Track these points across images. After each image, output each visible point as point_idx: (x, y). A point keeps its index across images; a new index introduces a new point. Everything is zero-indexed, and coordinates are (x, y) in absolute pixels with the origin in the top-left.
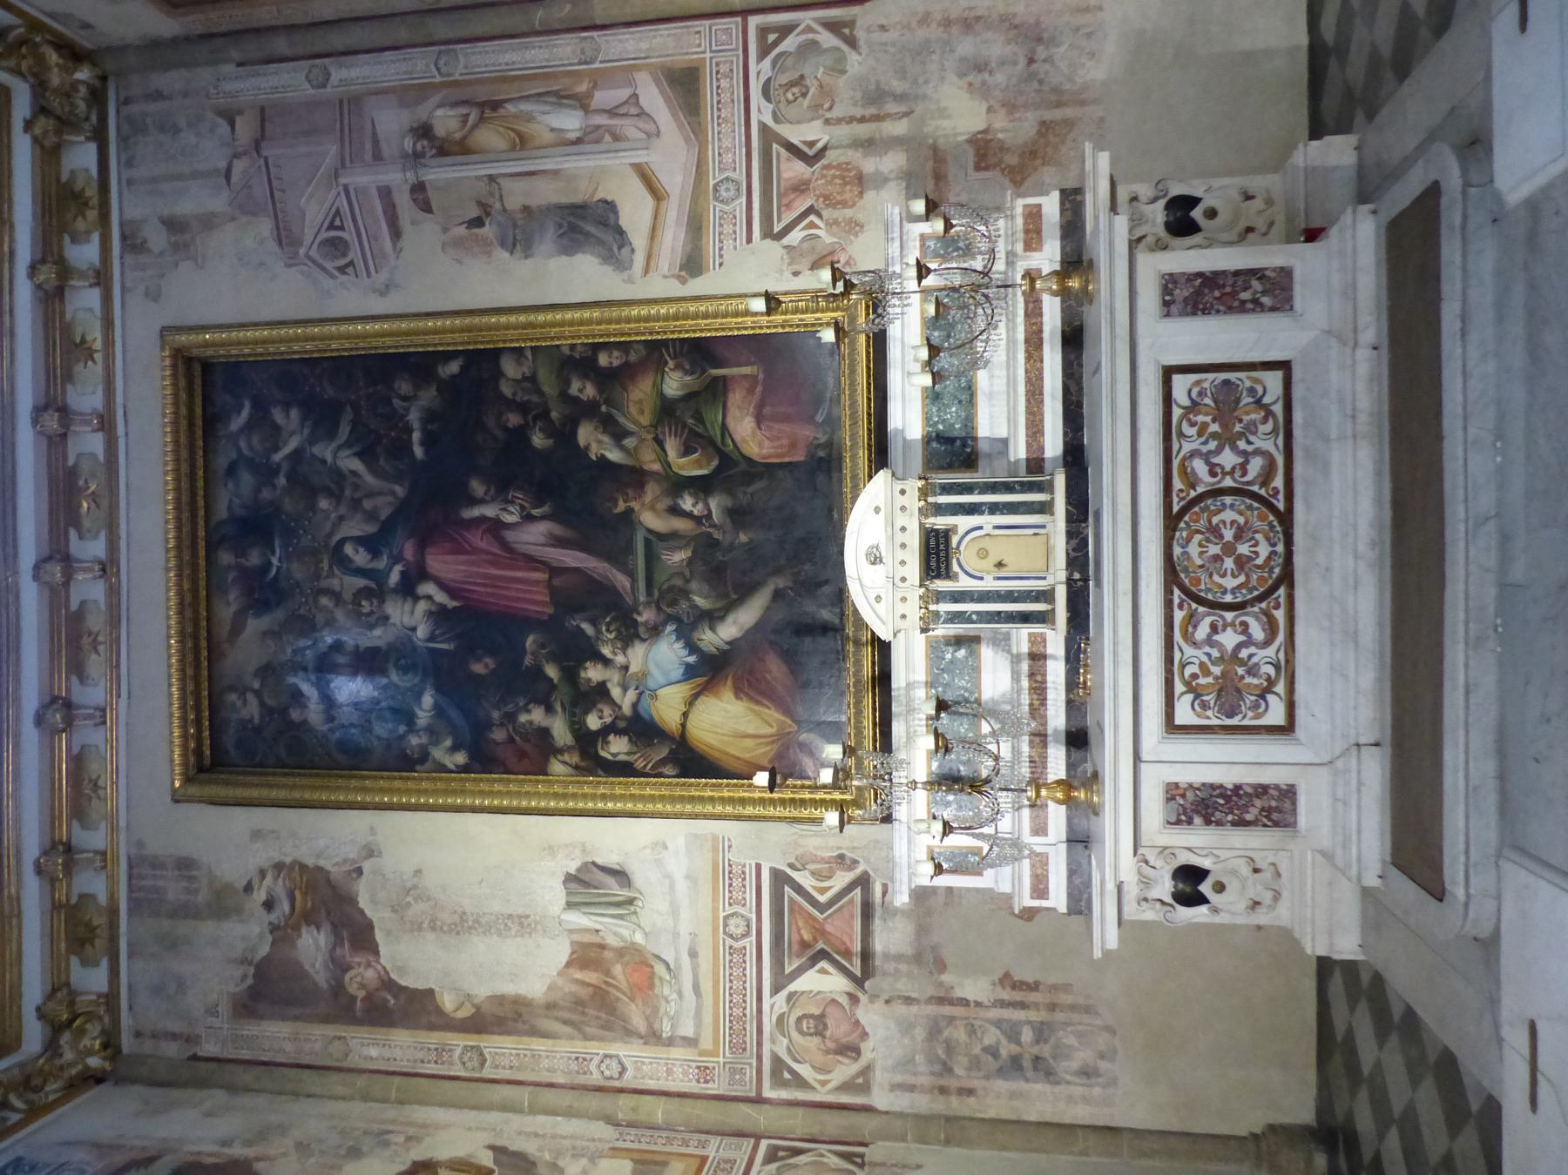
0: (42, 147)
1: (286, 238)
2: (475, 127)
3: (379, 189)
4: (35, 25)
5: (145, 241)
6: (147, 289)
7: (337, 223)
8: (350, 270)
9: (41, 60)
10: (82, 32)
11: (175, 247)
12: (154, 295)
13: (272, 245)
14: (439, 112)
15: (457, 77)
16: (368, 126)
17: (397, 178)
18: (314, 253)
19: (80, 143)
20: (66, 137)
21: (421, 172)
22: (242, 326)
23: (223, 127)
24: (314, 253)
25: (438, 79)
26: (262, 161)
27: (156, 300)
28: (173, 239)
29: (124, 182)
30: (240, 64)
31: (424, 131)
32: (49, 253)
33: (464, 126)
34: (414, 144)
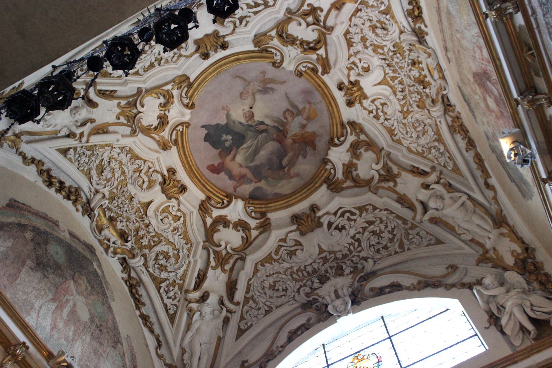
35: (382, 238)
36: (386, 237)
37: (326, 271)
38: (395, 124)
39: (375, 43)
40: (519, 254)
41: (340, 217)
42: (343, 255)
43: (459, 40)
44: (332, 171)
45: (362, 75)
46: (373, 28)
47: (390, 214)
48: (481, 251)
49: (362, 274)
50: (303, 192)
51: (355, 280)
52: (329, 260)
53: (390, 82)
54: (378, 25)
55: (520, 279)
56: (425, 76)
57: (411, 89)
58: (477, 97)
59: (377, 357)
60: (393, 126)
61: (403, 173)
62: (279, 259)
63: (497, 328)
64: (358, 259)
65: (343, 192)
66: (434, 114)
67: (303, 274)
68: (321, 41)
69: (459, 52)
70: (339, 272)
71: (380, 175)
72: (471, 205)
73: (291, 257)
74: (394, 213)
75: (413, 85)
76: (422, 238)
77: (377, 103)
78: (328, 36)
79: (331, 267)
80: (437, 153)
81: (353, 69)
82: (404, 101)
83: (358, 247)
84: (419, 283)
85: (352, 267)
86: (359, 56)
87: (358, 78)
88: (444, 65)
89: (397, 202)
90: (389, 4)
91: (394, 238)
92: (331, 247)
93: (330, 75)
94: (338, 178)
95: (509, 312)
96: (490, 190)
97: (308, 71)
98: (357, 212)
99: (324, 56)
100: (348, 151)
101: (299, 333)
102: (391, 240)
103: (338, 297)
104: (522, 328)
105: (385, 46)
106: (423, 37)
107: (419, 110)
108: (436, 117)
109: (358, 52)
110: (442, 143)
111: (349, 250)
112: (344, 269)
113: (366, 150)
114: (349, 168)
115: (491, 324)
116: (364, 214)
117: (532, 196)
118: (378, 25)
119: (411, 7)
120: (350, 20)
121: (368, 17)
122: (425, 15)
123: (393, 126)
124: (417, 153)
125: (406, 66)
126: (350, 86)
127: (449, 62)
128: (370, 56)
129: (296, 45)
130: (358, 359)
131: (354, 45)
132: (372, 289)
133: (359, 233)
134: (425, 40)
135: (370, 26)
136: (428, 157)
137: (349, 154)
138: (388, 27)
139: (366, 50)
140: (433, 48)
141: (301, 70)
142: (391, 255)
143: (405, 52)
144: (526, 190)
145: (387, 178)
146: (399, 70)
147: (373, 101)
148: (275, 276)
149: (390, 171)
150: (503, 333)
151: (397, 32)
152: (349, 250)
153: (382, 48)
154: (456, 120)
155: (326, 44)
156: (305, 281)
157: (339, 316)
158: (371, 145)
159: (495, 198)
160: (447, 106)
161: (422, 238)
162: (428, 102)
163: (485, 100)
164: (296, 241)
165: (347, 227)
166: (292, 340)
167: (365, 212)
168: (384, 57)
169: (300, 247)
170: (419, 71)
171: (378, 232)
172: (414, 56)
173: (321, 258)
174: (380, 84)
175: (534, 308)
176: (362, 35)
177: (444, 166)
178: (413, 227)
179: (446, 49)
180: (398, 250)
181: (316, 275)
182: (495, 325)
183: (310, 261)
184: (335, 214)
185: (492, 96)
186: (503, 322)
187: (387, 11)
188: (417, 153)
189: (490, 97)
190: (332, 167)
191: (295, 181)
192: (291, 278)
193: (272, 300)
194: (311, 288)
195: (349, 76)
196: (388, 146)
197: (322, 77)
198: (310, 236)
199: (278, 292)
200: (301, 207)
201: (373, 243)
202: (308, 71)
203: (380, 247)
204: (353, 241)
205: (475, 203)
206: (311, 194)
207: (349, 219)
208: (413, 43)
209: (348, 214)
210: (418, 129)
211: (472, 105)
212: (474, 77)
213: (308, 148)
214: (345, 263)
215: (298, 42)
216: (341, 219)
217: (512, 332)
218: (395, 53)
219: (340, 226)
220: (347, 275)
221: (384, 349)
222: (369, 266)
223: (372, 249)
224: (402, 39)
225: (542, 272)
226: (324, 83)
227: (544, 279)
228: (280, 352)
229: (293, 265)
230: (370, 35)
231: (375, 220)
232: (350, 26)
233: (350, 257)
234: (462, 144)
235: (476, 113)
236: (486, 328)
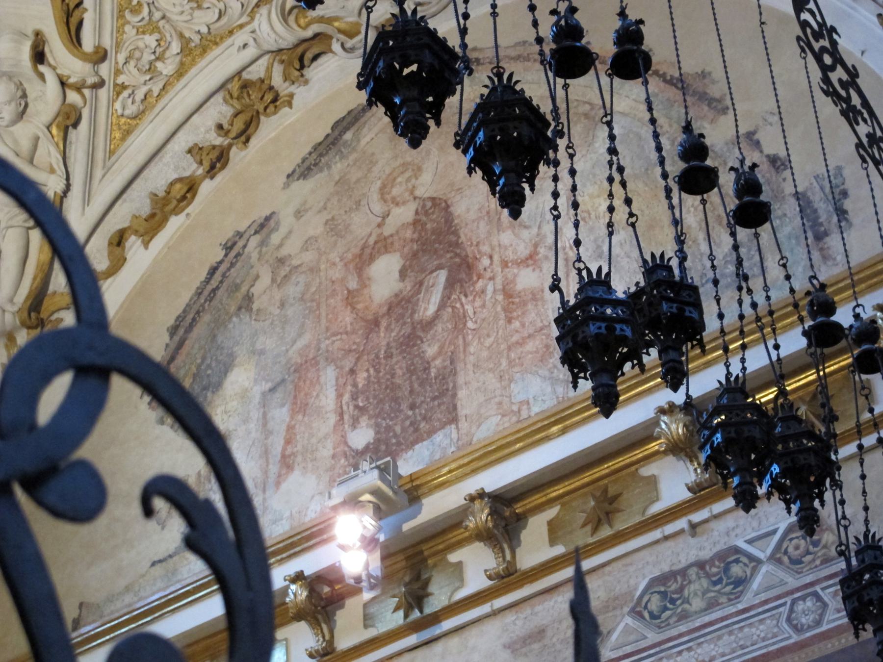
80: (148, 57)
96: (110, 254)
110: (182, 64)
136: (127, 28)
154: (269, 97)
163: (383, 245)
185: (408, 285)
189: (403, 274)
235: (318, 179)
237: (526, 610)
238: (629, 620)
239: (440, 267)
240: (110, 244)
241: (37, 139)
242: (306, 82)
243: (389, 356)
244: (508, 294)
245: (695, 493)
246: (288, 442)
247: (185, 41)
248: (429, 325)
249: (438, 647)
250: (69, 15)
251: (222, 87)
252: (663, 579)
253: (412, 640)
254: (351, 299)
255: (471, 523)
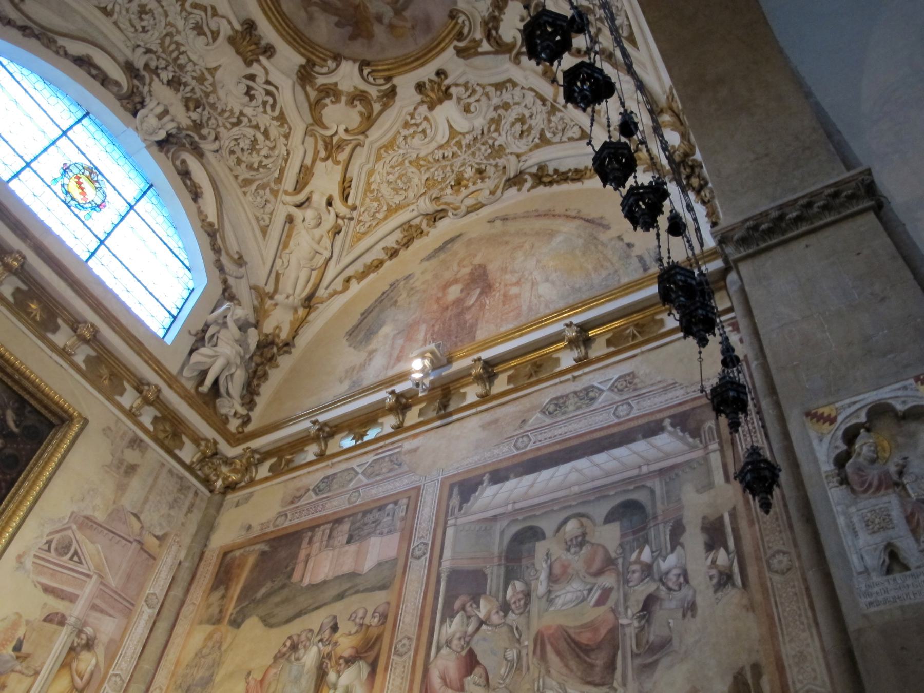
0: (202, 439)
1: (87, 523)
2: (73, 680)
3: (77, 596)
4: (252, 482)
5: (134, 449)
6: (112, 431)
7: (76, 558)
8: (46, 547)
9: (235, 471)
10: (236, 499)
11: (121, 462)
12: (107, 431)
13: (89, 513)
14: (94, 662)
15: (106, 685)
16: (112, 612)
17: (74, 612)
18: (69, 533)
19: (193, 458)
20: (200, 454)
21: (70, 628)
22: (59, 465)
23: (159, 533)
24: (69, 533)
25: (111, 672)
26: (132, 540)
27: (104, 430)
28: (125, 464)
29: (165, 462)
30: (180, 563)
31: (89, 645)
32: (157, 401)
33: (77, 671)
34: (87, 634)
35: (250, 154)
36: (253, 160)
37: (186, 84)
38: (401, 152)
39: (503, 122)
40: (278, 336)
41: (265, 90)
42: (214, 103)
43: (522, 247)
44: (325, 70)
45: (459, 103)
46: (521, 120)
47: (283, 158)
48: (270, 288)
49: (196, 138)
50: (290, 32)
51: (187, 129)
52: (202, 84)
53: (454, 141)
54: (525, 127)
55: (253, 346)
56: (466, 187)
57: (448, 169)
58: (455, 268)
59: (103, 201)
60: (399, 148)
61: (339, 169)
62: (186, 11)
63: (194, 345)
64: (214, 126)
65: (298, 88)
66: (421, 200)
67: (173, 51)
68: (501, 48)
69: (507, 243)
70: (192, 105)
71: (331, 136)
72: (320, 264)
73: (194, 29)
74: (286, 163)
75: (453, 172)
76: (263, 207)
77: (425, 125)
78: (507, 56)
79: (193, 90)
80: (373, 210)
81: (467, 90)
82: (431, 160)
83: (231, 123)
84: (211, 225)
85: (201, 122)
86: (484, 99)
87: (454, 97)
88: (484, 212)
89: (302, 166)
90: (553, 143)
91: (254, 170)
92: (220, 85)
93: (455, 57)
94: (316, 78)
95: (217, 354)
96: (344, 285)
97: (458, 27)
98: (277, 113)
99: (480, 50)
100: (355, 88)
101: (94, 72)
102: (250, 167)
103: (160, 117)
104: (204, 374)
105: (500, 135)
106: (515, 185)
107: (423, 181)
108: (418, 203)
109: (489, 98)
111: (223, 111)
112: (197, 110)
113: (361, 114)
114: (331, 92)
115: (195, 335)
116: (275, 123)
117: (354, 347)
118: (525, 127)
119: (551, 172)
120: (531, 89)
121: (535, 113)
122: (541, 190)
123: (399, 148)
124: (369, 184)
125: (478, 161)
126: (443, 88)
127: (489, 222)
128: (486, 113)
129: (494, 11)
130: (91, 174)
131: (498, 93)
132: (184, 162)
133: (250, 121)
134: (511, 187)
135: (524, 116)
136: (367, 199)
137: (352, 89)
138: (524, 141)
139: (492, 108)
140: (503, 197)
141: (458, 18)
142: (231, 170)
143: (494, 159)
144: (359, 338)
145: (329, 146)
146: (470, 152)
147: (426, 118)
148: (160, 10)
149: (340, 150)
150: (191, 352)
151: (519, 151)
152: (223, 111)
153: (497, 130)
154: (419, 231)
155: (496, 53)
156: (164, 56)
157: (136, 129)
158: (369, 120)
159: (335, 293)
160: (435, 217)
161: (263, 207)
162: (435, 193)
163: (456, 281)
164: (218, 32)
165: (254, 103)
166: (80, 66)
167: (279, 123)
168: (485, 132)
169: (211, 40)
170: (471, 177)
171: (257, 147)
172: (491, 171)
173: (203, 74)
174: (450, 127)
175: (229, 378)
176: (511, 104)
177: (359, 222)
178: (275, 193)
179: (505, 219)
180: (241, 178)
181: (177, 70)
182: (196, 341)
183: (194, 58)
184: (268, 82)
185: (463, 295)
186: (203, 350)
187: (544, 141)
188: (369, 184)
189: (462, 291)
190: (331, 69)
191: (303, 14)
192: (162, 35)
193: (124, 12)
194: (157, 68)
195: (457, 85)
196: (372, 143)
197: (451, 47)
198: (230, 51)
199: (138, 20)
200: (267, 32)
201: (242, 145)
202: (458, 27)
203: (239, 153)
204: (237, 114)
205: (324, 266)
206: (289, 43)
207: (265, 103)
208: (507, 173)
209: (271, 100)
210: (399, 182)
211: (442, 256)
212: (480, 266)
213: (349, 29)
214: (204, 109)
215: (497, 14)
216: (264, 93)
217: (195, 363)
218: (492, 146)
219: (252, 92)
220: (190, 117)
221: (116, 206)
222: (207, 147)
223: (233, 143)
224: (509, 156)
225: (267, 368)
226: (443, 50)
227: (260, 373)
228: (57, 53)
229: (183, 34)
230: (513, 114)
231: (272, 139)
232: (522, 88)
233: (214, 114)
234: (391, 242)
235: (434, 261)
236: (190, 332)
237: (492, 412)
238: (539, 415)
239: (478, 288)
240: (344, 281)
241: (322, 236)
242: (435, 227)
243: (450, 319)
244: (505, 296)
245: (577, 362)
246: (401, 352)
247: (389, 206)
248: (469, 308)
249: (449, 427)
250: (344, 190)
251: (401, 226)
252: (557, 398)
253: (439, 423)
254: (438, 300)
255: (473, 372)
